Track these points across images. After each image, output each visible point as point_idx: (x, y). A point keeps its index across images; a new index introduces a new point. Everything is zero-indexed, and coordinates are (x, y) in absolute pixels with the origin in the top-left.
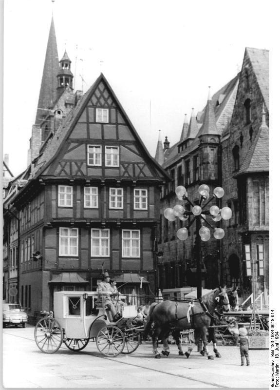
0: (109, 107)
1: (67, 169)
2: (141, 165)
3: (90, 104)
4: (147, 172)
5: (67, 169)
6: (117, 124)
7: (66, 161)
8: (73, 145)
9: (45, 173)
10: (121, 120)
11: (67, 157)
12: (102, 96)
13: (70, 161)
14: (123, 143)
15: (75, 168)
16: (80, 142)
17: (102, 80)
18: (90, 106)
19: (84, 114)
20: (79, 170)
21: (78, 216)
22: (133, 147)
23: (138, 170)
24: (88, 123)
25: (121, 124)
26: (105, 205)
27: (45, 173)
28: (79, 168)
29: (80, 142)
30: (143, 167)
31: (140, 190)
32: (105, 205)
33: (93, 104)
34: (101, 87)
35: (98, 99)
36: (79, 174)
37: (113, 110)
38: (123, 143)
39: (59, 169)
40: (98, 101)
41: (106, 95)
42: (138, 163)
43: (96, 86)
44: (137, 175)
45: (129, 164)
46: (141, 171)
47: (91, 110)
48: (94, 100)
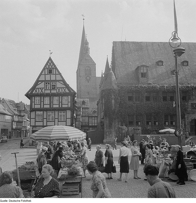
3: (46, 68)
4: (67, 91)
5: (37, 91)
6: (56, 74)
7: (37, 88)
8: (39, 83)
9: (29, 93)
10: (57, 73)
12: (50, 65)
13: (39, 88)
15: (40, 91)
17: (50, 59)
19: (44, 71)
20: (42, 91)
21: (42, 107)
23: (63, 90)
24: (45, 75)
25: (58, 74)
26: (52, 103)
27: (29, 93)
28: (42, 90)
29: (42, 81)
32: (52, 103)
33: (47, 68)
34: (50, 62)
35: (49, 66)
37: (54, 70)
38: (59, 81)
39: (35, 91)
41: (52, 64)
42: (63, 88)
43: (48, 62)
45: (60, 88)
47: (46, 70)
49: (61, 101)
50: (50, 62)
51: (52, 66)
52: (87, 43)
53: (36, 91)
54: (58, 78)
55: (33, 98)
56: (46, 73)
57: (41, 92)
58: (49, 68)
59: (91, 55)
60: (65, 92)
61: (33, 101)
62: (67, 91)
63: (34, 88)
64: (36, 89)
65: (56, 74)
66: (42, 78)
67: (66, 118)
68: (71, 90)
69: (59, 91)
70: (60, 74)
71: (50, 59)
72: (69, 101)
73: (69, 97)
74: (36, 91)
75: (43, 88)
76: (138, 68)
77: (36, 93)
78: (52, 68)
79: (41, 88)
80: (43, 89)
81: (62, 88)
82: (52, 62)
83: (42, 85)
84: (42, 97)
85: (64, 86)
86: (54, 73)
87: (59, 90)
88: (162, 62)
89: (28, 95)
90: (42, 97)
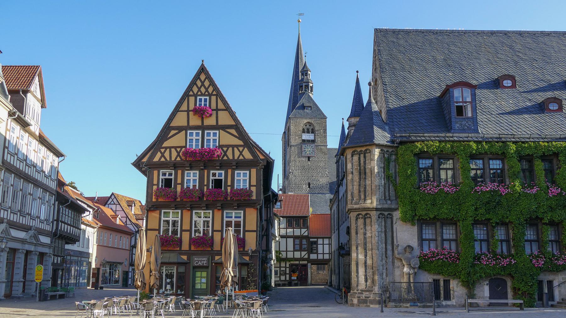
0: (210, 95)
1: (167, 154)
2: (241, 149)
3: (191, 93)
4: (247, 155)
5: (167, 154)
7: (166, 148)
8: (173, 132)
9: (145, 160)
10: (221, 106)
11: (165, 144)
12: (203, 85)
13: (170, 148)
14: (224, 128)
15: (174, 154)
16: (180, 129)
17: (203, 69)
18: (191, 96)
20: (178, 155)
22: (233, 131)
24: (188, 111)
29: (180, 129)
30: (243, 150)
31: (242, 172)
33: (193, 92)
35: (199, 89)
36: (178, 159)
37: (214, 98)
38: (224, 128)
39: (159, 155)
40: (199, 89)
41: (207, 83)
42: (237, 146)
43: (197, 77)
44: (236, 158)
45: (228, 146)
46: (241, 153)
47: (192, 99)
48: (195, 89)
49: (229, 183)
50: (203, 77)
51: (207, 90)
52: (305, 72)
53: (163, 155)
54: (225, 118)
55: (155, 172)
56: (192, 107)
57: (176, 158)
58: (199, 93)
59: (314, 96)
60: (241, 157)
61: (155, 182)
62: (247, 155)
63: (156, 146)
64: (163, 150)
65: (217, 110)
66: (181, 120)
67: (245, 231)
68: (258, 153)
69: (225, 154)
70: (228, 108)
71: (203, 69)
72: (254, 182)
73: (254, 171)
74: (163, 155)
75: (181, 147)
76: (447, 91)
77: (163, 159)
78: (208, 92)
79: (175, 148)
80: (180, 151)
81: (233, 146)
82: (209, 77)
83: (177, 140)
84: (180, 172)
85: (241, 143)
86: (214, 106)
87: (225, 153)
88: (512, 78)
89: (138, 164)
90: (180, 172)
